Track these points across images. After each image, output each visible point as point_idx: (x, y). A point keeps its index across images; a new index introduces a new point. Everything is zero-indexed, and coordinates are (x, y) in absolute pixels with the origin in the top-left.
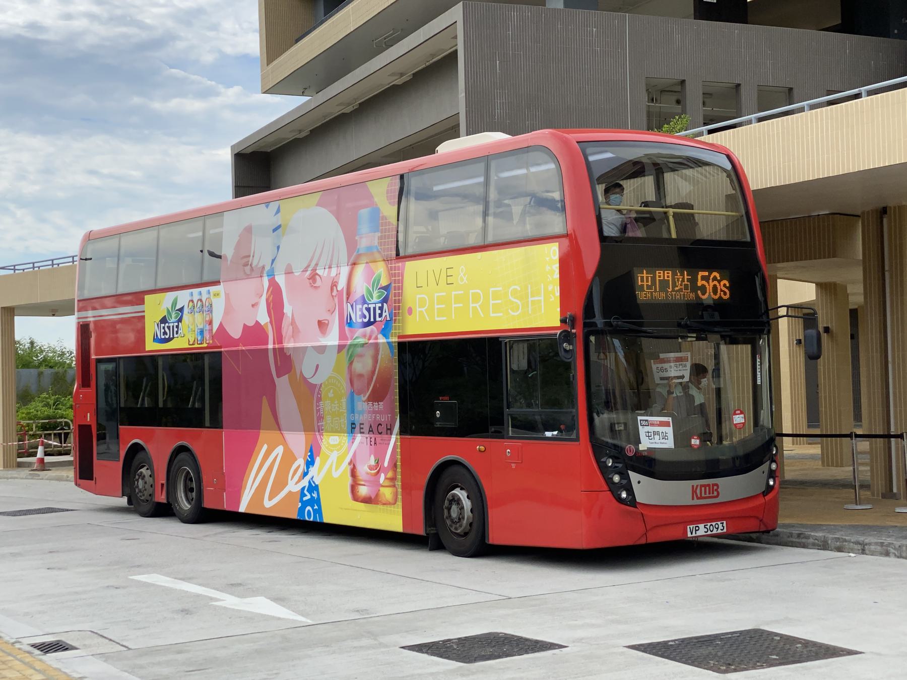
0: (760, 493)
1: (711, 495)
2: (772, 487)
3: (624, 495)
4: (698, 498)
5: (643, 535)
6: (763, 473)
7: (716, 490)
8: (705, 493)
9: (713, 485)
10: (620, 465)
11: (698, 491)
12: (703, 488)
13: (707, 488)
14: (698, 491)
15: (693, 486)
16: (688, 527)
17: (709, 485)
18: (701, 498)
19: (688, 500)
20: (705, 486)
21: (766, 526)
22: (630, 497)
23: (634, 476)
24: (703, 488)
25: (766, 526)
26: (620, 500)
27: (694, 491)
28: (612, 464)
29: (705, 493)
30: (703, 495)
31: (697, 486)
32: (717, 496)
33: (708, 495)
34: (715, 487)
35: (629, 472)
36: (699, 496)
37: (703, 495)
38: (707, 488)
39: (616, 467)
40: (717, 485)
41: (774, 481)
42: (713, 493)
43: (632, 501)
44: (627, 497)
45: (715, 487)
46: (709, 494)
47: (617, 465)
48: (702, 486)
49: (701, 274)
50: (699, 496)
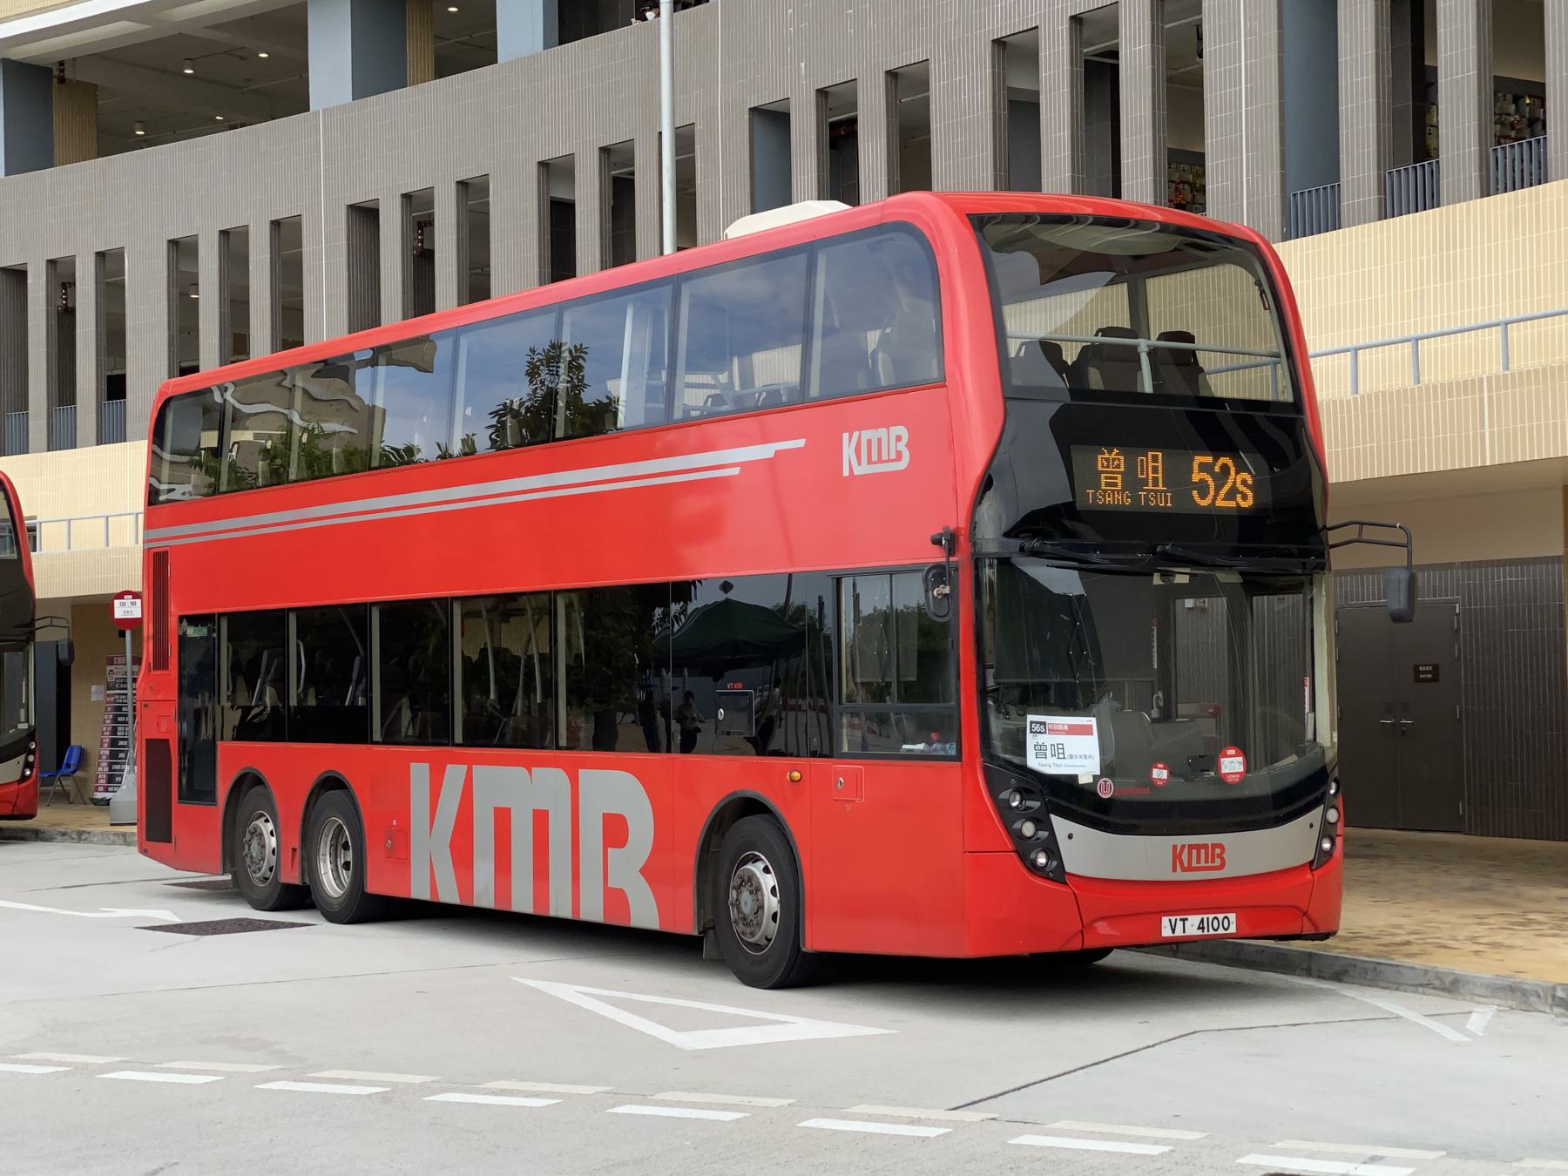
0: (1304, 865)
1: (1210, 864)
2: (1329, 853)
3: (1042, 860)
4: (1184, 869)
5: (1077, 934)
6: (1311, 826)
7: (1220, 856)
8: (1199, 861)
9: (1215, 846)
10: (1036, 804)
13: (1203, 851)
15: (1175, 847)
16: (1165, 920)
17: (1205, 846)
18: (1190, 869)
19: (1165, 873)
20: (1198, 847)
21: (1315, 926)
22: (1055, 863)
23: (1060, 825)
25: (1315, 926)
26: (1033, 868)
27: (1177, 856)
28: (1021, 803)
29: (1199, 861)
30: (1194, 864)
31: (1183, 847)
32: (1221, 867)
33: (1203, 864)
34: (1218, 851)
35: (1052, 815)
36: (1186, 865)
37: (1194, 864)
38: (1203, 851)
39: (1028, 808)
40: (1221, 846)
41: (1333, 843)
42: (1213, 861)
43: (1058, 874)
44: (1047, 863)
45: (1218, 851)
46: (1206, 862)
47: (1029, 803)
48: (1191, 847)
49: (1199, 459)
50: (1186, 865)
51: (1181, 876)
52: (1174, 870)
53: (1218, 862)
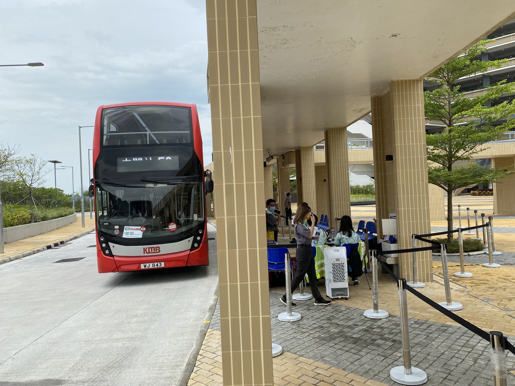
1: (155, 251)
4: (147, 253)
8: (152, 251)
9: (156, 247)
11: (147, 250)
12: (150, 249)
13: (153, 249)
14: (147, 250)
15: (144, 248)
17: (154, 248)
18: (149, 253)
20: (151, 248)
24: (150, 249)
27: (145, 250)
29: (152, 251)
31: (147, 248)
33: (153, 251)
34: (158, 248)
37: (150, 252)
38: (153, 249)
42: (156, 251)
46: (154, 251)
48: (149, 248)
51: (146, 254)
52: (144, 253)
53: (158, 251)
